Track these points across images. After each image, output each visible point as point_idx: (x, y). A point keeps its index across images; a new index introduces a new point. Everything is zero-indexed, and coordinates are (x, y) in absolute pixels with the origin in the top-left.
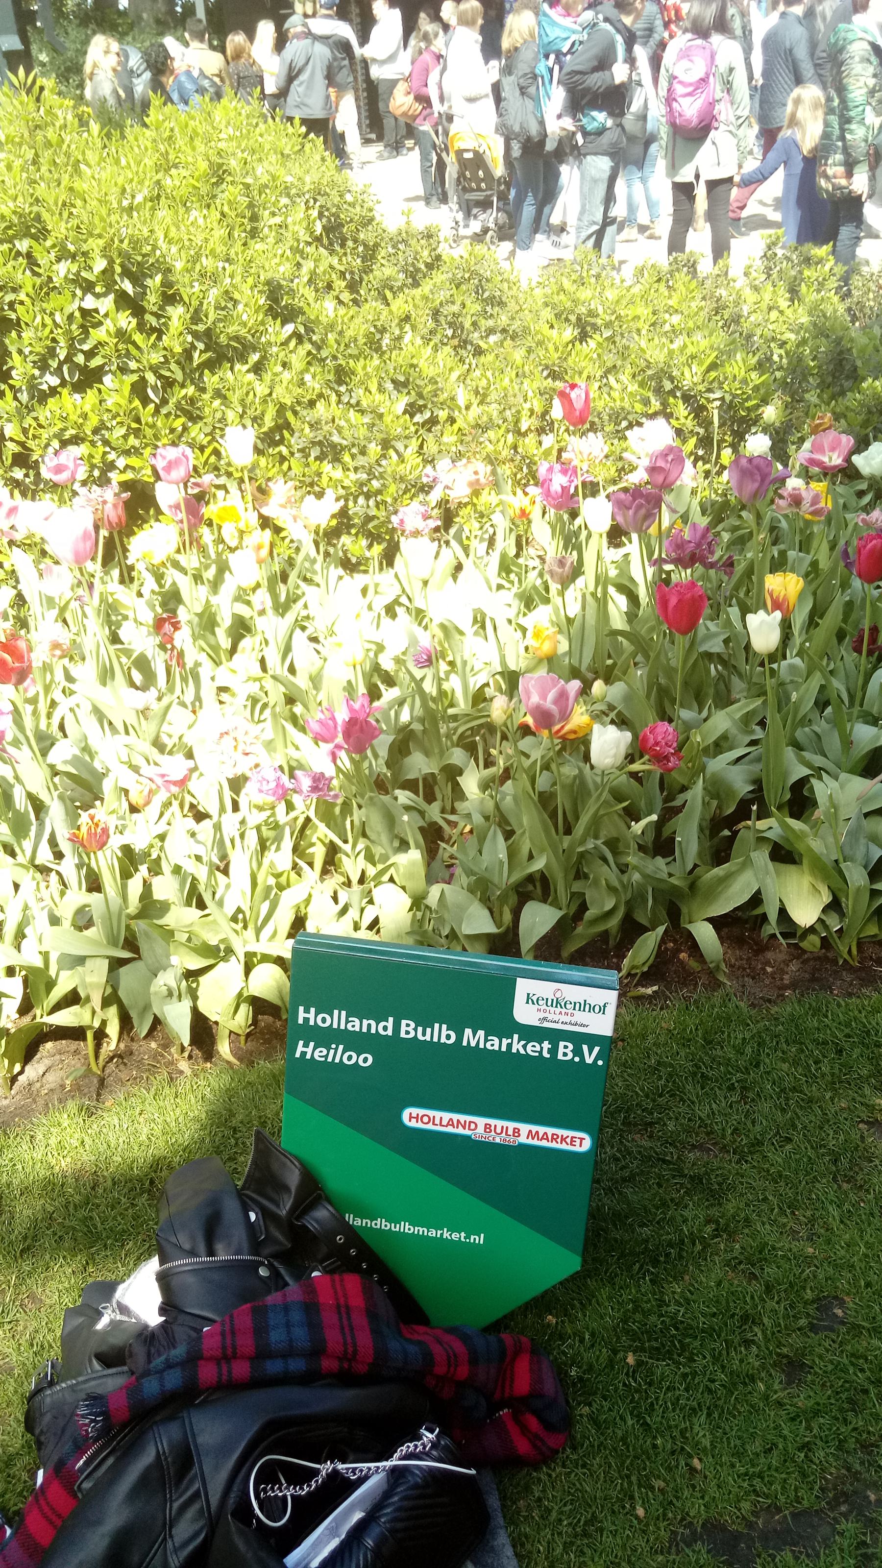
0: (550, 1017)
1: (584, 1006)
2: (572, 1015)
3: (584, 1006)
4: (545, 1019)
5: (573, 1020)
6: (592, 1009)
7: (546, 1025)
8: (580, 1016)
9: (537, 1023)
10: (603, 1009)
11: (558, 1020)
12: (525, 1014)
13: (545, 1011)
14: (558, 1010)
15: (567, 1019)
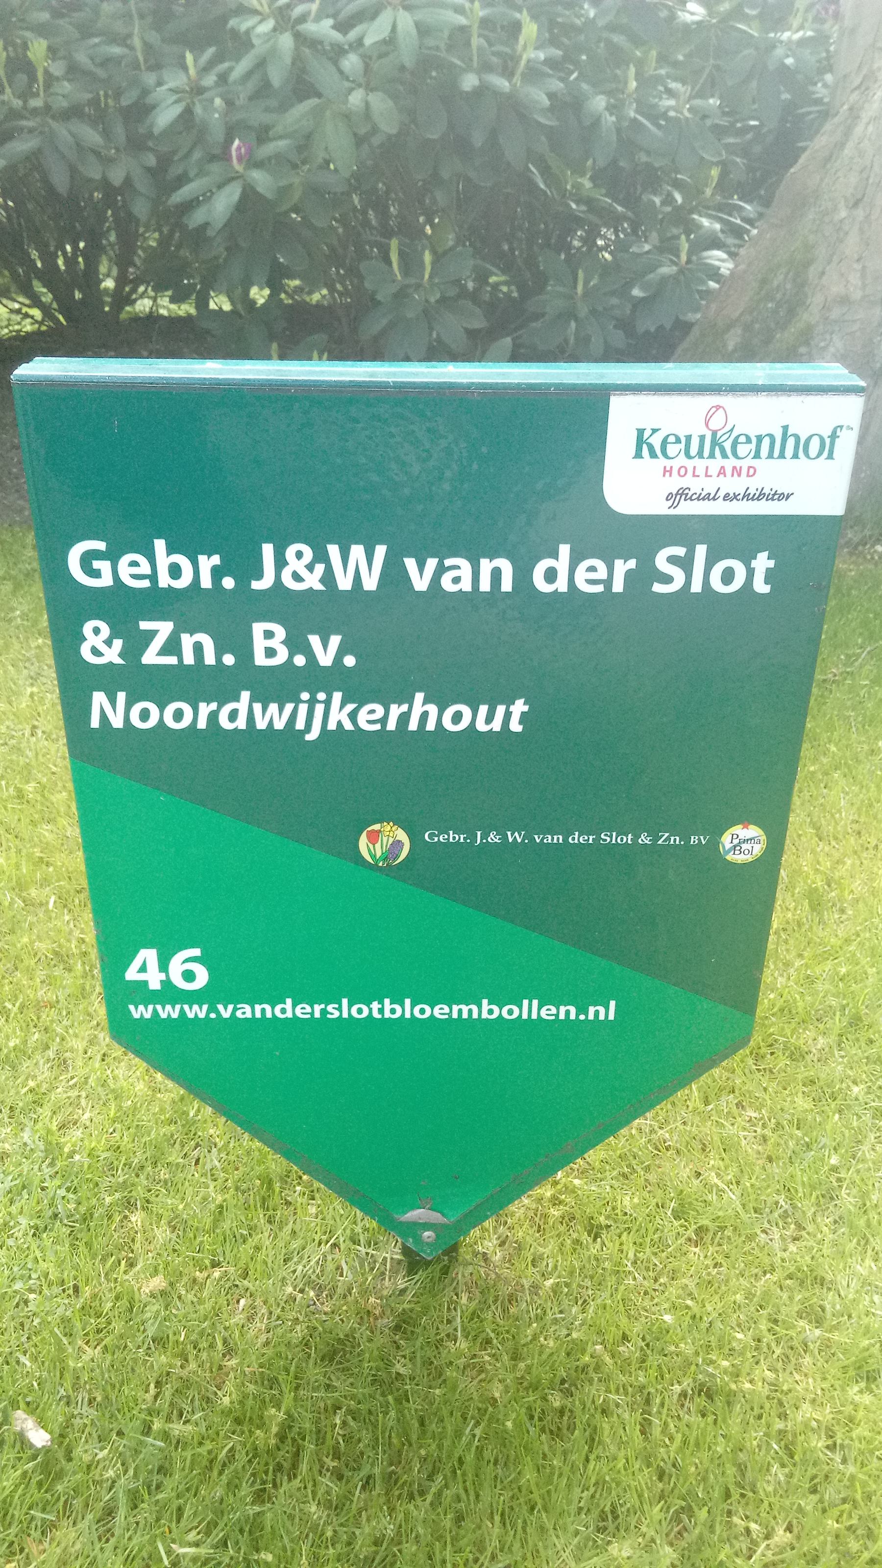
0: (696, 486)
1: (785, 444)
2: (752, 472)
3: (785, 444)
4: (683, 494)
5: (753, 485)
6: (802, 448)
7: (686, 508)
8: (771, 474)
9: (662, 508)
10: (828, 447)
11: (719, 490)
12: (631, 486)
13: (683, 472)
14: (718, 462)
15: (737, 485)
